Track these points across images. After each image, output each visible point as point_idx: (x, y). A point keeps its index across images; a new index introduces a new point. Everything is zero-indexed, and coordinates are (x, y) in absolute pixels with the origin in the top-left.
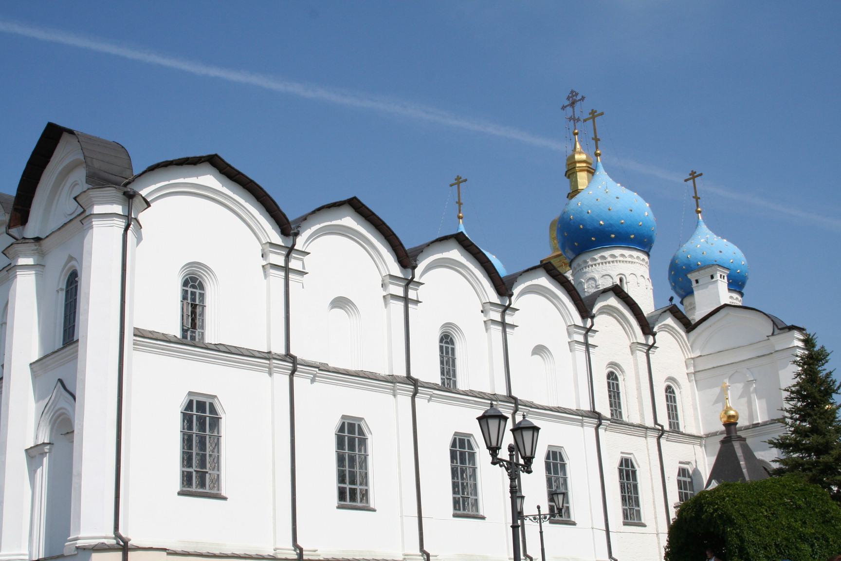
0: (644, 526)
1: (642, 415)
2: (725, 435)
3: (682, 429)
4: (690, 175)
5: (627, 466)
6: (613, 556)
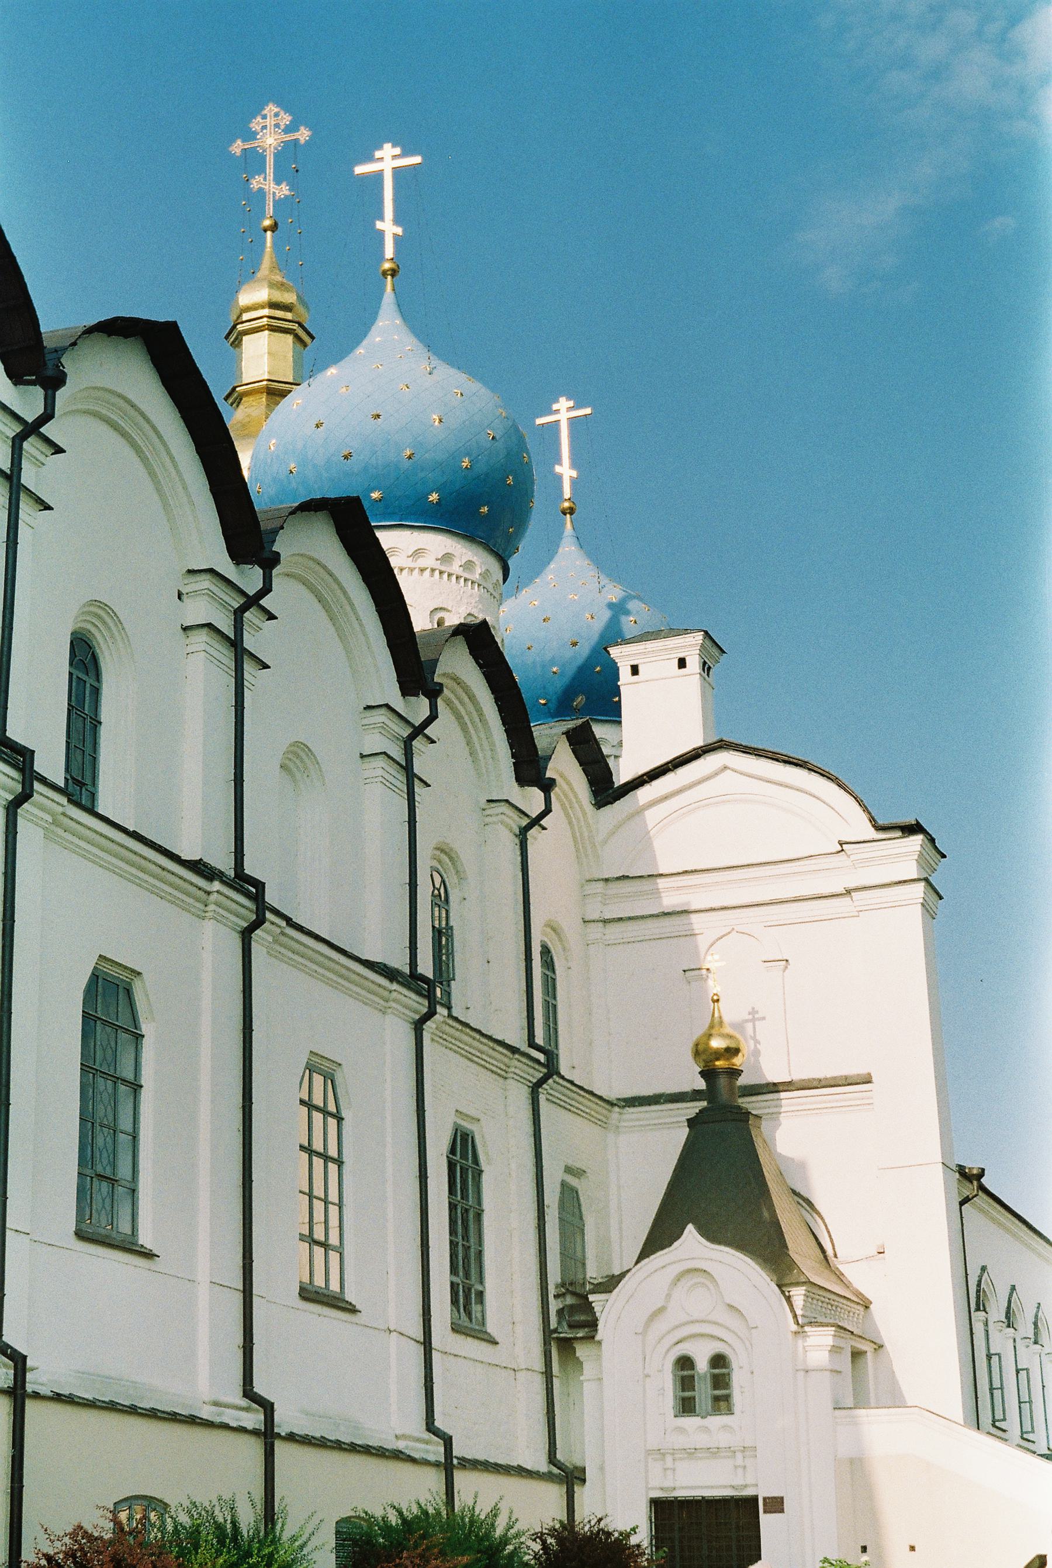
5: (464, 1156)
6: (438, 1423)
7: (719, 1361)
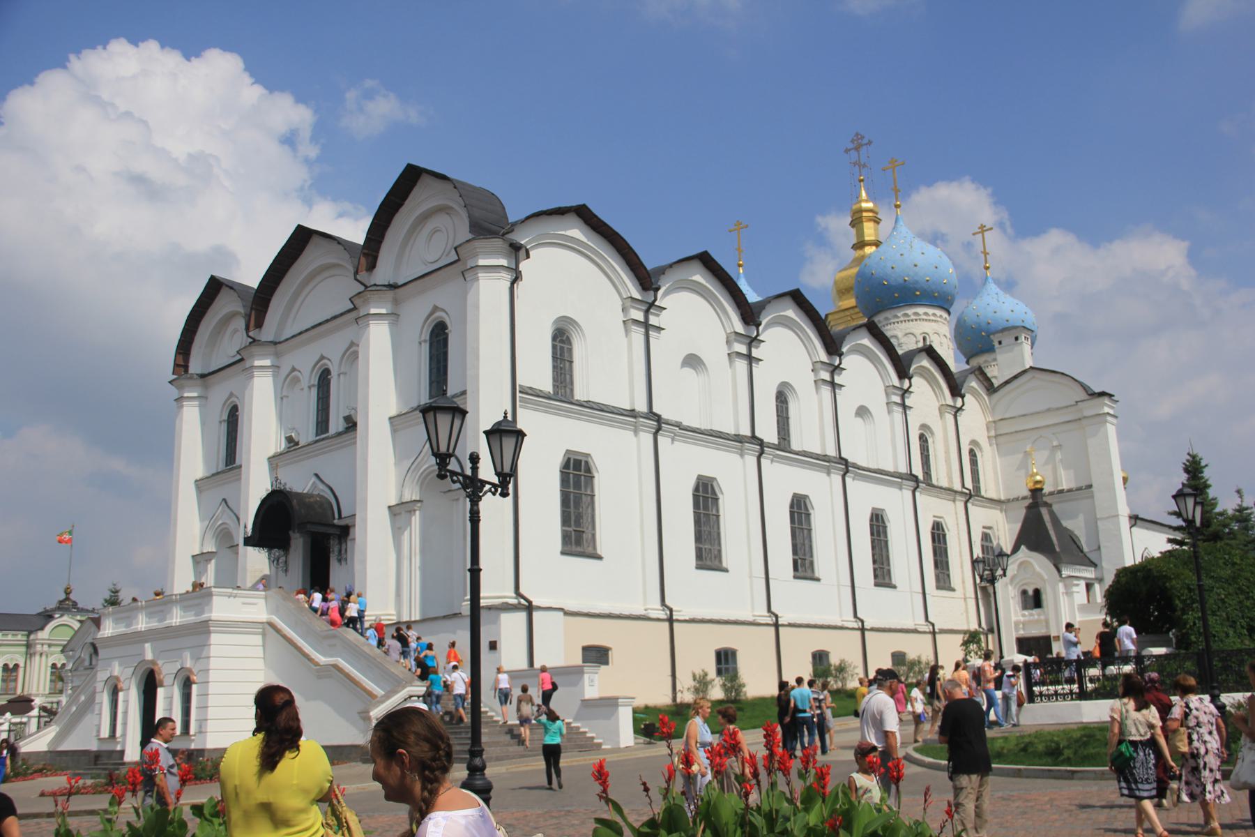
0: (953, 590)
1: (950, 479)
2: (1030, 501)
3: (983, 493)
4: (979, 228)
5: (938, 529)
7: (1037, 592)
